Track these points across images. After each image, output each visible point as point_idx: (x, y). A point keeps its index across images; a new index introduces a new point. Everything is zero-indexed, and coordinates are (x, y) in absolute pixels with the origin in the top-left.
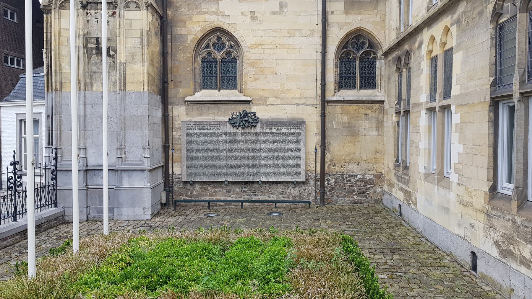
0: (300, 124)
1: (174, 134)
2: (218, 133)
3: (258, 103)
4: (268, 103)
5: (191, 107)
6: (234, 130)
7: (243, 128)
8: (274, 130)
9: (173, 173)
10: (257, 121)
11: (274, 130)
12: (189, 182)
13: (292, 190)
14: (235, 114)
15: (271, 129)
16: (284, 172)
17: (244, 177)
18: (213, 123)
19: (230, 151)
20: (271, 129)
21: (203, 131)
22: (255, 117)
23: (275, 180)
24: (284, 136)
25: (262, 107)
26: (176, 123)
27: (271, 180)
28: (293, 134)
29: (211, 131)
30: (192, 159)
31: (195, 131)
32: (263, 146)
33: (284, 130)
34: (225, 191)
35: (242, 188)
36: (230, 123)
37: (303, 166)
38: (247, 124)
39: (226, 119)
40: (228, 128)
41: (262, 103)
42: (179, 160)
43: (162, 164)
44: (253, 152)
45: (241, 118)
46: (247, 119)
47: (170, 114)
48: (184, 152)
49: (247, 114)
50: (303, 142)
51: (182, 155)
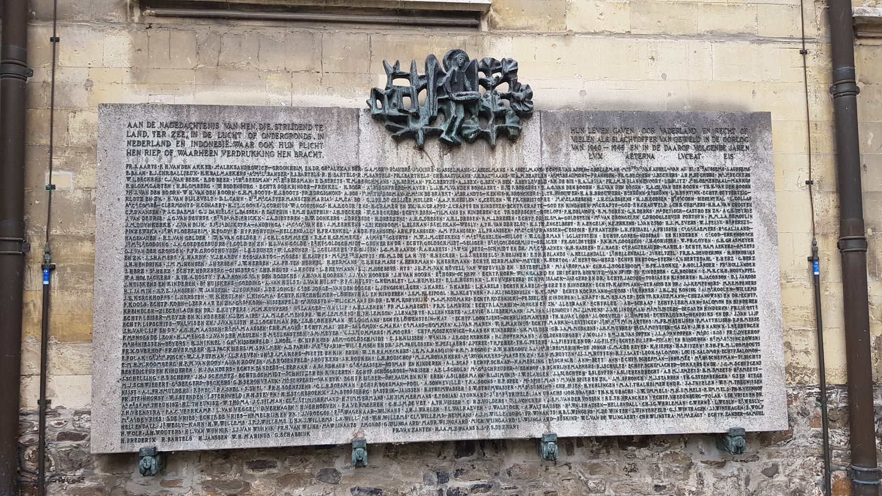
0: (745, 128)
1: (62, 179)
3: (520, 23)
4: (571, 24)
5: (163, 34)
6: (403, 156)
7: (450, 146)
8: (614, 159)
9: (44, 402)
10: (522, 106)
11: (614, 159)
13: (709, 478)
15: (596, 152)
16: (673, 380)
17: (458, 419)
18: (283, 118)
19: (380, 271)
20: (596, 152)
21: (225, 161)
22: (516, 86)
23: (626, 428)
24: (664, 191)
25: (543, 43)
27: (606, 429)
28: (709, 175)
29: (271, 162)
30: (155, 321)
31: (178, 160)
32: (559, 241)
33: (667, 158)
35: (443, 478)
38: (474, 125)
41: (541, 24)
44: (505, 275)
45: (439, 90)
46: (470, 94)
48: (113, 281)
49: (468, 70)
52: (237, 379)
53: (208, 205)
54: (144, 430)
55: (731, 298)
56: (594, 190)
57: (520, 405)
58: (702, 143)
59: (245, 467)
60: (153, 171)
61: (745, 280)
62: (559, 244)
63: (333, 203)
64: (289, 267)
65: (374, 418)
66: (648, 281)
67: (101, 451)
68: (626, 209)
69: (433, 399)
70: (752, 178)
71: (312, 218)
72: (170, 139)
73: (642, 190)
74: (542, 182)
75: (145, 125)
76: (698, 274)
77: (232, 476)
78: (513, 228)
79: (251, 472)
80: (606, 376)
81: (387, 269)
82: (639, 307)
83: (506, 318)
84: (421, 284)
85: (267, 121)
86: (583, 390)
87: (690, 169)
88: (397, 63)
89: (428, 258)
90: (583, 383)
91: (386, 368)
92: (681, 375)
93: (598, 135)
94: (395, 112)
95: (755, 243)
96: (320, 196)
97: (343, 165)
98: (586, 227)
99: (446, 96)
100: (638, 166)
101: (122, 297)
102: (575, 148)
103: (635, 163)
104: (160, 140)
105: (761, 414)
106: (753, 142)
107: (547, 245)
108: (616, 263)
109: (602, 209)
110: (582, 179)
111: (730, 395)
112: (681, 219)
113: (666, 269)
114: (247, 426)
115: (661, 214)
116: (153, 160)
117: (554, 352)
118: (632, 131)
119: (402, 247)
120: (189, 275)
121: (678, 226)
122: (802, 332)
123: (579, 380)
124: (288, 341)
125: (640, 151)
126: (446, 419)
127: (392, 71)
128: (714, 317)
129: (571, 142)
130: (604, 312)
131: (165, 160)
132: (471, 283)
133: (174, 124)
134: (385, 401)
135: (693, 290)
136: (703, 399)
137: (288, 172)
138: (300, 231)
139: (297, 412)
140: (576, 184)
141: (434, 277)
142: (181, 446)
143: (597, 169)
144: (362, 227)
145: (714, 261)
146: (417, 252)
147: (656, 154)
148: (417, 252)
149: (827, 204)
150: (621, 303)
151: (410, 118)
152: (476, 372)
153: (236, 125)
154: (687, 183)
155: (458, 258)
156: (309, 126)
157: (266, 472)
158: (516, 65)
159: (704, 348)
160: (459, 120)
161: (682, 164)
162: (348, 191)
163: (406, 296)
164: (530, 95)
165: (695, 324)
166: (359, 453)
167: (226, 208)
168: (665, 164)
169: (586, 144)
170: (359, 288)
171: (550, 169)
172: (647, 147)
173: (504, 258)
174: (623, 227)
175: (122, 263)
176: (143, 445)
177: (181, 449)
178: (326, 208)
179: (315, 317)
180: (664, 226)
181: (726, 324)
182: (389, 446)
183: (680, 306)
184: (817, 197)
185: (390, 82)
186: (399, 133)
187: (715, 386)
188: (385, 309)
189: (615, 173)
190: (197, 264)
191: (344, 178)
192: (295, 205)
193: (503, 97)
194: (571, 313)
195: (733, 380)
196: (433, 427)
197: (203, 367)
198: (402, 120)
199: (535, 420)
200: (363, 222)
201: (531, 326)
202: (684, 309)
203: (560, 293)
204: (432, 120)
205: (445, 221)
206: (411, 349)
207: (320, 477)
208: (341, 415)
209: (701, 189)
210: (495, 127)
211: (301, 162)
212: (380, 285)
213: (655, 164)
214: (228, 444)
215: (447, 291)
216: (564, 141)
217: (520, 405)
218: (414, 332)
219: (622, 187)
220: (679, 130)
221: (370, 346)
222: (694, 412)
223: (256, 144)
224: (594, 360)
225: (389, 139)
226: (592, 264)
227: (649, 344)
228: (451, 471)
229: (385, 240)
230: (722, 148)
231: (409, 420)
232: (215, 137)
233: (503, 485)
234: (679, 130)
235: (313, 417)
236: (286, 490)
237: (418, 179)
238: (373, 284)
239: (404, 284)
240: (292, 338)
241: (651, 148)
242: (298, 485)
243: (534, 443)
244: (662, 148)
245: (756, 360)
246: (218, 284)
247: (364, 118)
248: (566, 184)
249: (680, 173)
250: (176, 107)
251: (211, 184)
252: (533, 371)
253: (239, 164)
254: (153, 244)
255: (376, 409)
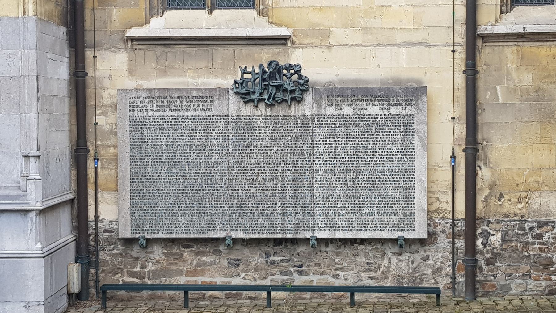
0: (414, 93)
2: (207, 118)
6: (248, 110)
7: (270, 106)
8: (347, 110)
10: (304, 86)
11: (347, 110)
12: (137, 239)
14: (249, 69)
15: (339, 107)
18: (195, 94)
19: (238, 162)
20: (339, 107)
22: (300, 77)
23: (349, 235)
24: (373, 126)
26: (105, 94)
27: (340, 235)
28: (393, 118)
30: (143, 183)
31: (151, 113)
32: (320, 149)
33: (373, 110)
34: (225, 263)
36: (237, 93)
37: (420, 200)
38: (280, 96)
39: (228, 83)
40: (234, 106)
42: (113, 186)
43: (71, 196)
44: (295, 165)
45: (264, 80)
46: (279, 82)
47: (90, 72)
48: (125, 166)
49: (278, 69)
50: (421, 139)
51: (120, 174)
52: (177, 209)
53: (163, 133)
54: (140, 229)
55: (402, 177)
56: (337, 125)
57: (300, 223)
58: (391, 102)
59: (181, 247)
60: (141, 118)
61: (409, 168)
62: (320, 151)
63: (217, 132)
64: (198, 160)
65: (235, 227)
66: (362, 168)
67: (123, 237)
68: (353, 134)
69: (261, 220)
70: (415, 119)
71: (208, 139)
72: (147, 104)
73: (361, 125)
74: (313, 122)
75: (136, 98)
76: (386, 165)
77: (175, 251)
78: (299, 143)
79: (183, 249)
80: (341, 212)
81: (241, 162)
82: (357, 180)
83: (295, 184)
84: (256, 169)
85: (188, 95)
86: (330, 217)
87: (385, 115)
88: (246, 67)
89: (259, 157)
90: (330, 214)
91: (240, 205)
92: (376, 211)
93: (340, 99)
94: (244, 91)
95: (415, 150)
96: (211, 129)
97: (221, 114)
98: (333, 143)
99: (267, 83)
100: (359, 113)
101: (129, 173)
102: (329, 105)
103: (358, 112)
104: (143, 105)
105: (414, 230)
106: (417, 101)
107: (315, 151)
108: (347, 159)
109: (341, 134)
110: (332, 120)
111: (400, 221)
112: (379, 139)
113: (371, 162)
114: (182, 228)
115: (369, 136)
116: (140, 114)
117: (317, 200)
118: (357, 96)
119: (248, 151)
120: (156, 164)
121: (377, 142)
122: (445, 193)
123: (328, 213)
124: (198, 193)
125: (360, 106)
126: (267, 228)
127: (243, 72)
128: (393, 185)
129: (327, 102)
130: (341, 182)
131: (145, 113)
132: (279, 168)
133: (148, 97)
134: (240, 220)
135: (384, 172)
136: (386, 222)
137: (197, 118)
138: (203, 144)
139: (202, 223)
140: (329, 122)
141: (262, 165)
142: (155, 236)
143: (339, 115)
144: (230, 143)
145: (394, 159)
146: (254, 154)
147: (368, 108)
148: (254, 154)
149: (461, 129)
150: (348, 178)
151: (251, 93)
152: (281, 208)
153: (175, 97)
154: (383, 122)
155: (273, 157)
156: (206, 97)
157: (190, 249)
158: (301, 67)
159: (387, 199)
160: (273, 94)
161: (380, 112)
162: (224, 126)
163: (249, 174)
164: (307, 81)
165: (384, 188)
166: (229, 241)
167: (171, 135)
168: (372, 112)
169: (334, 103)
170: (228, 170)
171: (317, 115)
172: (363, 105)
173: (295, 157)
174: (351, 143)
175: (129, 158)
176: (140, 235)
177: (155, 237)
178: (214, 134)
179: (210, 183)
180: (371, 142)
181: (399, 188)
182: (243, 240)
183: (377, 180)
184: (457, 126)
185: (242, 76)
186: (246, 100)
187: (392, 217)
188: (240, 180)
189: (348, 117)
190: (160, 159)
191: (222, 121)
192: (200, 132)
193: (294, 82)
194: (325, 183)
195: (401, 214)
196: (261, 232)
197: (163, 203)
198: (248, 94)
199: (307, 230)
200: (230, 140)
201: (306, 188)
202: (379, 181)
203: (320, 173)
204: (261, 94)
205: (267, 140)
206: (252, 197)
207: (213, 253)
208: (221, 225)
209: (390, 125)
210: (290, 96)
211: (203, 114)
212: (238, 169)
213: (367, 112)
214: (174, 236)
215: (268, 172)
216: (324, 102)
217: (300, 223)
218: (253, 190)
219: (351, 124)
220: (380, 96)
221: (233, 196)
222: (381, 229)
223: (183, 106)
224: (335, 204)
225: (242, 102)
226: (336, 160)
227: (362, 197)
228: (272, 253)
229: (240, 148)
230: (401, 105)
231: (251, 228)
232: (166, 103)
233: (296, 260)
234: (380, 96)
235: (210, 225)
236: (199, 257)
237: (255, 121)
238: (235, 169)
239: (249, 168)
240: (200, 192)
241: (365, 105)
242: (204, 256)
243: (307, 240)
244: (371, 105)
245: (413, 205)
246: (168, 168)
247: (231, 93)
248: (324, 122)
249: (379, 117)
250: (150, 90)
251: (165, 124)
252: (307, 209)
253: (176, 115)
254: (141, 150)
255: (236, 223)
